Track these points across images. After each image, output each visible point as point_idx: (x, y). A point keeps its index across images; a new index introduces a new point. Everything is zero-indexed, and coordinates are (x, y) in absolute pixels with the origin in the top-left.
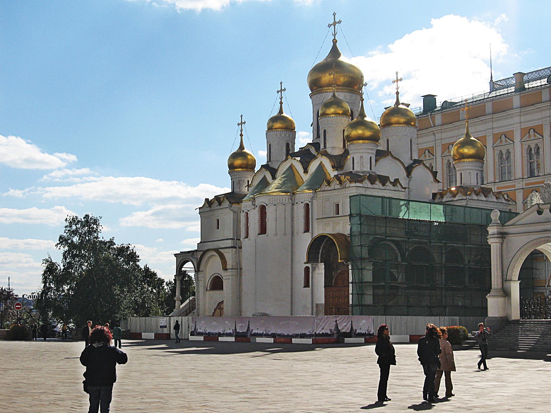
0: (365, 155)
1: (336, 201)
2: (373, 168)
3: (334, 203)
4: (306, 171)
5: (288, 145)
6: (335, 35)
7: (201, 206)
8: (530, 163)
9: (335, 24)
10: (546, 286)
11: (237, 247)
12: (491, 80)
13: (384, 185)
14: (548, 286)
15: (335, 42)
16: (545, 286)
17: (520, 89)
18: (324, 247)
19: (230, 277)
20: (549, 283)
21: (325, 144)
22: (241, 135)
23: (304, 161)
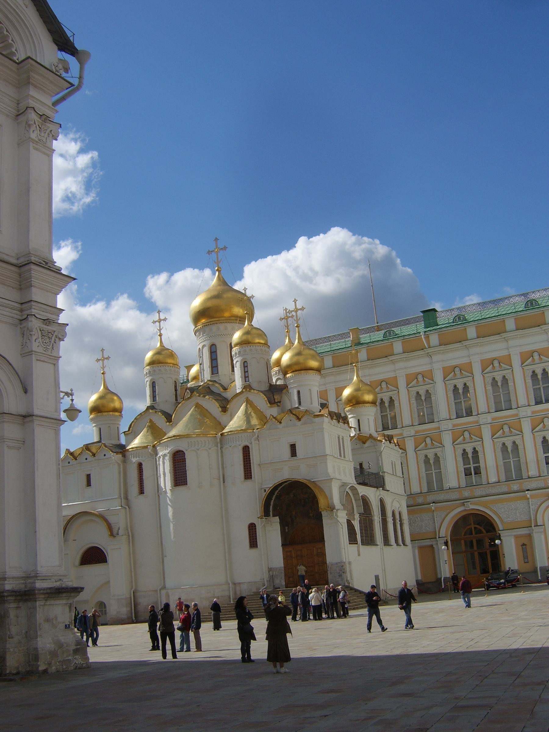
3: (288, 443)
4: (224, 409)
8: (381, 416)
10: (437, 537)
13: (339, 422)
14: (439, 537)
16: (436, 538)
20: (439, 535)
23: (216, 399)
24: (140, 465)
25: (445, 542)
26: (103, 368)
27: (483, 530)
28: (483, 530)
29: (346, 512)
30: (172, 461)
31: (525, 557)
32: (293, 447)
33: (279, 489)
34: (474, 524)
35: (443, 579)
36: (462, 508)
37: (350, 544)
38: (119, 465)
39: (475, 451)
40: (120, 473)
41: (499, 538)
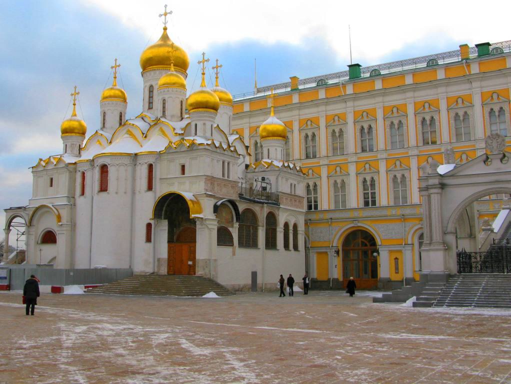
0: (207, 122)
1: (182, 162)
2: (213, 135)
5: (121, 113)
6: (165, 23)
7: (35, 166)
9: (166, 14)
10: (331, 246)
11: (73, 206)
12: (256, 87)
14: (332, 246)
15: (165, 29)
17: (295, 90)
18: (168, 206)
19: (64, 232)
20: (332, 244)
21: (164, 112)
22: (74, 105)
24: (83, 174)
25: (335, 251)
26: (75, 100)
27: (368, 244)
28: (368, 244)
29: (217, 221)
30: (100, 172)
31: (397, 269)
32: (183, 167)
33: (170, 199)
34: (362, 239)
35: (331, 279)
36: (353, 225)
37: (218, 245)
38: (70, 172)
39: (373, 180)
40: (70, 178)
41: (378, 252)
